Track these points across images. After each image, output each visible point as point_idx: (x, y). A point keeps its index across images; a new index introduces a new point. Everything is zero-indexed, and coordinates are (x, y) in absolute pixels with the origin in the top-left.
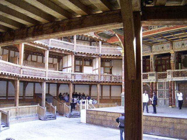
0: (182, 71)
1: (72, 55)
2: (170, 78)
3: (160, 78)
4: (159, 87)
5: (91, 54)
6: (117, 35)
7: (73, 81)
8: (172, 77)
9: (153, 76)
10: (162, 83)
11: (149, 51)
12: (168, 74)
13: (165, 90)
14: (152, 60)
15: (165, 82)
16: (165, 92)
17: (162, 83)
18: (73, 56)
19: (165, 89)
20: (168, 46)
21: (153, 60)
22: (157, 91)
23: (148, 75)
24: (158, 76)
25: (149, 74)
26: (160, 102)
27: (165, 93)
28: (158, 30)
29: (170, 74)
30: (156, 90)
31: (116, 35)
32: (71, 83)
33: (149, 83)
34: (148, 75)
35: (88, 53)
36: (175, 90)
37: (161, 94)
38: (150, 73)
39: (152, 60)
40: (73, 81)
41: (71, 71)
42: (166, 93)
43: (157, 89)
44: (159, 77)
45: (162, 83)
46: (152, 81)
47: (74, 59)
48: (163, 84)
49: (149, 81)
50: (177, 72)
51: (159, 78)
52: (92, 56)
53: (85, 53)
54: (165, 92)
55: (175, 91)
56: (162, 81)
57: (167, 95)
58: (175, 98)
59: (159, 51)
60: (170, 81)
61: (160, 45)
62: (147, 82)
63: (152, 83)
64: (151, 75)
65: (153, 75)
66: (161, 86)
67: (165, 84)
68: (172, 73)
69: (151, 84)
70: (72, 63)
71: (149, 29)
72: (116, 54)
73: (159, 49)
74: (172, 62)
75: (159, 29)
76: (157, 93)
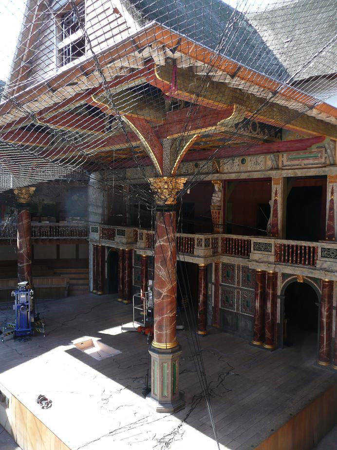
22: (133, 269)
43: (133, 265)
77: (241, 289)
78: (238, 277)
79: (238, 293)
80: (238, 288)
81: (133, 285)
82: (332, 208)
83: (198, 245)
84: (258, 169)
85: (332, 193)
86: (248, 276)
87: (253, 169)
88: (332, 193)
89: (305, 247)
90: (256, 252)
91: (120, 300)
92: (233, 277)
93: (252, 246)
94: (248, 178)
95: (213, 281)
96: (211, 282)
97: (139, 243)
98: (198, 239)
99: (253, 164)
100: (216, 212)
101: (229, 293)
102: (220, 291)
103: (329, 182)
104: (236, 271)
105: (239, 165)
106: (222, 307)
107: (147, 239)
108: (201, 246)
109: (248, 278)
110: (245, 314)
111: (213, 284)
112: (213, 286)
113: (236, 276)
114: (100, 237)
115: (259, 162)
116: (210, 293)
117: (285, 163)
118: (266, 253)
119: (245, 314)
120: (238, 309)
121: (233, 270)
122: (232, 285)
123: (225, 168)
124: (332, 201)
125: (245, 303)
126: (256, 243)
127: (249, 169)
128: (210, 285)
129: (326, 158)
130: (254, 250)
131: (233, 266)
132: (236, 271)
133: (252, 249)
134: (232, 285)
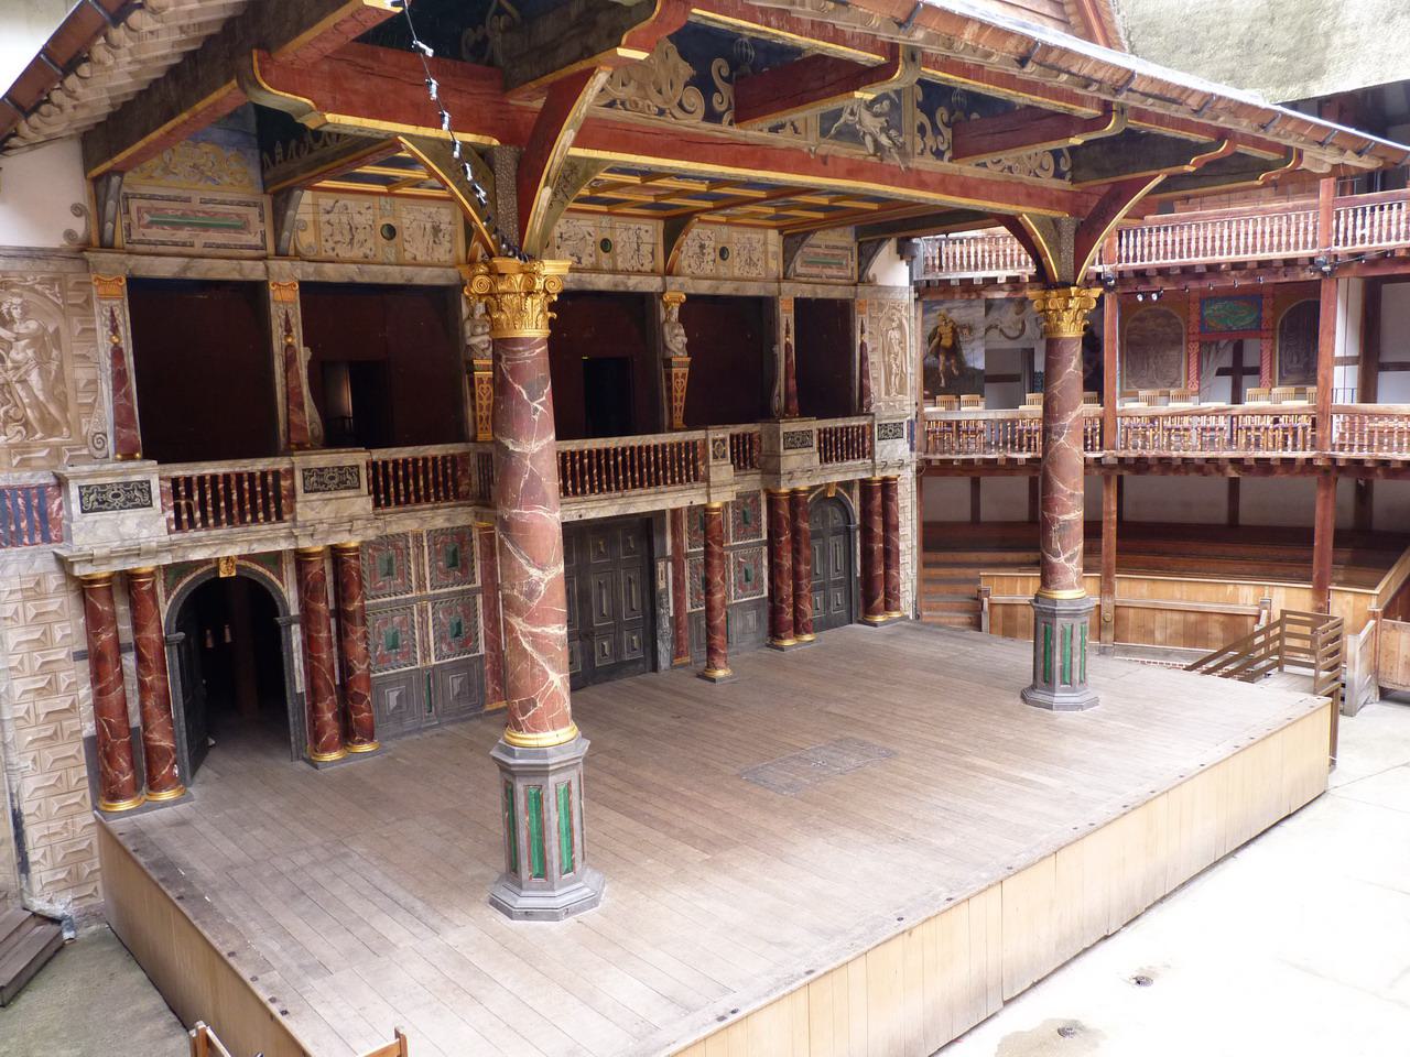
0: (599, 451)
9: (343, 485)
10: (396, 547)
11: (256, 240)
13: (428, 598)
14: (288, 330)
15: (418, 537)
16: (422, 611)
17: (396, 547)
19: (421, 586)
20: (436, 230)
21: (298, 331)
26: (393, 703)
27: (424, 623)
28: (824, 159)
38: (313, 465)
39: (288, 330)
48: (403, 553)
54: (422, 611)
57: (440, 639)
59: (357, 253)
61: (367, 201)
64: (320, 482)
66: (389, 573)
67: (420, 547)
73: (359, 236)
82: (864, 358)
83: (715, 457)
85: (862, 332)
86: (744, 513)
88: (862, 332)
89: (853, 427)
90: (789, 452)
94: (734, 293)
95: (669, 552)
96: (664, 557)
103: (860, 313)
105: (714, 261)
106: (692, 607)
108: (724, 456)
109: (745, 518)
111: (667, 559)
112: (670, 564)
114: (170, 532)
115: (755, 260)
116: (661, 585)
117: (800, 270)
118: (805, 450)
123: (685, 264)
124: (863, 345)
127: (737, 273)
128: (661, 566)
129: (852, 269)
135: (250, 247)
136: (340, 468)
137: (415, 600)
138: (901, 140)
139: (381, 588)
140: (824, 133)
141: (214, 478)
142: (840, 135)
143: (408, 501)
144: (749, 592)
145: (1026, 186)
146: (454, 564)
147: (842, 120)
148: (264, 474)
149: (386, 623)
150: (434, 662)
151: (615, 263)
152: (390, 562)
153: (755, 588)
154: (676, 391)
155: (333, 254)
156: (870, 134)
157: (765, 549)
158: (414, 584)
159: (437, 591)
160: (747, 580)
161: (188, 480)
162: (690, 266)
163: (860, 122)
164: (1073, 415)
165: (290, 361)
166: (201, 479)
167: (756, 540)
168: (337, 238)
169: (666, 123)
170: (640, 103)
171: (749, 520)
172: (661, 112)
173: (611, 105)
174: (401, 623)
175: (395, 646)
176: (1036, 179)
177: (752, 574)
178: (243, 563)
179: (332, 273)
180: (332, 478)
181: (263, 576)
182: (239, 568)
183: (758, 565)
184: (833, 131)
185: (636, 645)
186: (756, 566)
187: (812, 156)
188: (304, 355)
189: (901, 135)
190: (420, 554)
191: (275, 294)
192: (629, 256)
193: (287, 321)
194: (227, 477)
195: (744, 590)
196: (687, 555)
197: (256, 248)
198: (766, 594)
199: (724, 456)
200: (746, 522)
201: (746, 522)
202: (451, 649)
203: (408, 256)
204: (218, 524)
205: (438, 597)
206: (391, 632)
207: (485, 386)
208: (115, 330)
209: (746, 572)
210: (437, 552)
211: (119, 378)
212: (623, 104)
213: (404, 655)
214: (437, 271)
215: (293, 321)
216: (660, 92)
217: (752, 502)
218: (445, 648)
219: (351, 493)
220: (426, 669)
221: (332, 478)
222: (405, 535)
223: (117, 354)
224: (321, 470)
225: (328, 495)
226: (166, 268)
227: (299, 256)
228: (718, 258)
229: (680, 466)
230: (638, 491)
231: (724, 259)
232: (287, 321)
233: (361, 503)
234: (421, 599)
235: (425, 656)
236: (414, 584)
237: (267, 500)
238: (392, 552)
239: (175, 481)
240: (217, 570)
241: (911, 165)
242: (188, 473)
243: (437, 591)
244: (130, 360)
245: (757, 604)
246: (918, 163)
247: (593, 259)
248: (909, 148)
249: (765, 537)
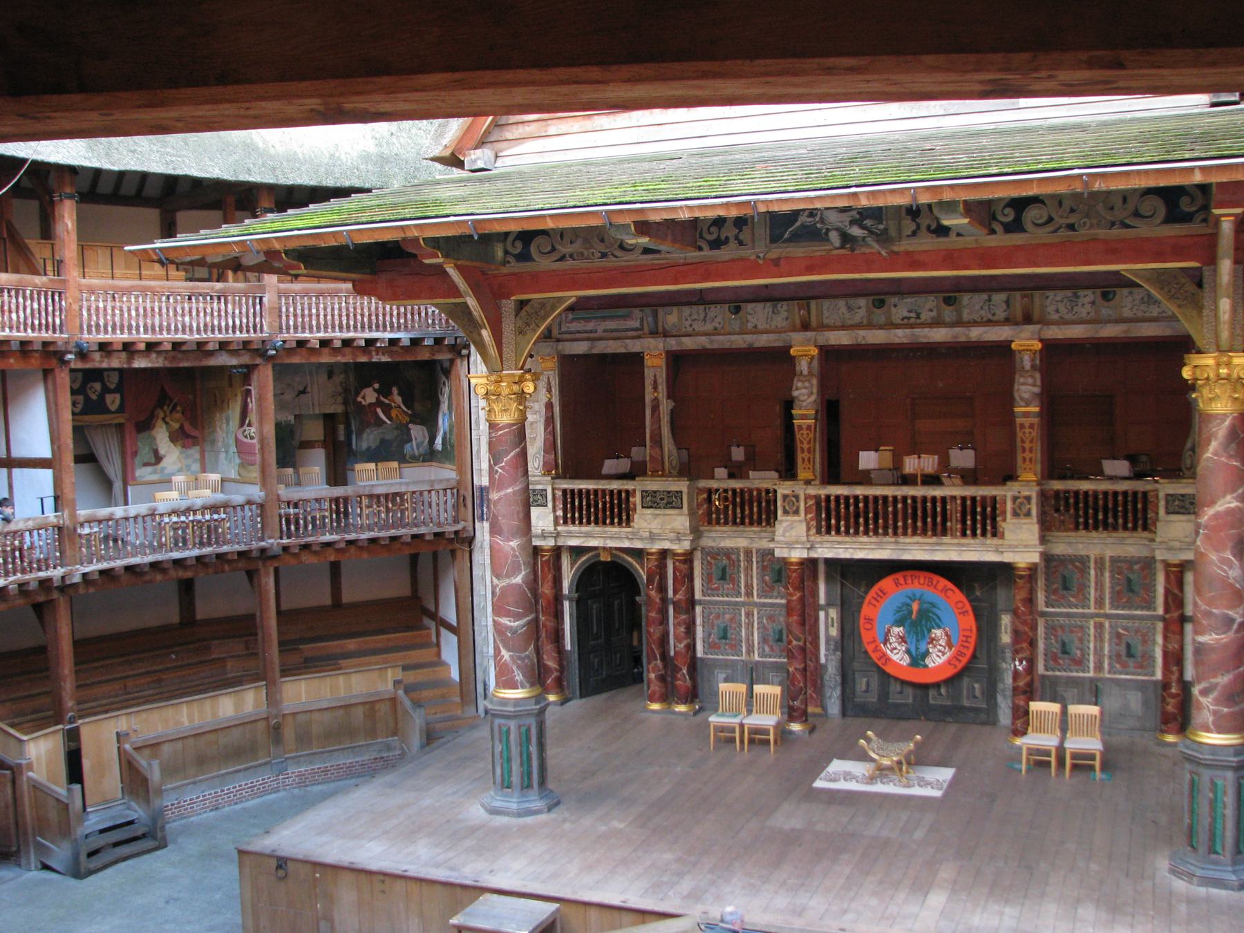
1: (47, 373)
2: (793, 538)
3: (718, 523)
4: (708, 578)
5: (201, 344)
6: (458, 267)
7: (77, 579)
8: (808, 529)
9: (669, 505)
10: (729, 558)
11: (637, 324)
12: (786, 512)
13: (756, 604)
14: (655, 388)
15: (748, 553)
17: (729, 558)
18: (63, 378)
19: (749, 594)
21: (662, 388)
22: (698, 609)
23: (637, 499)
24: (699, 506)
25: (638, 495)
27: (750, 625)
28: (776, 263)
29: (796, 512)
30: (691, 603)
31: (451, 271)
32: (55, 595)
33: (638, 554)
34: (637, 499)
35: (176, 345)
36: (824, 608)
37: (725, 630)
39: (655, 388)
40: (77, 579)
41: (49, 503)
42: (762, 627)
43: (698, 596)
44: (709, 513)
45: (728, 553)
46: (666, 545)
47: (66, 400)
48: (735, 564)
49: (638, 545)
50: (847, 498)
51: (710, 523)
52: (212, 362)
53: (151, 346)
55: (822, 614)
56: (728, 543)
57: (764, 640)
58: (823, 660)
59: (709, 327)
60: (797, 554)
62: (626, 544)
63: (664, 553)
64: (654, 501)
65: (670, 501)
66: (723, 578)
67: (749, 561)
68: (811, 502)
69: (653, 563)
70: (55, 438)
71: (705, 246)
72: (388, 335)
74: (804, 417)
75: (776, 252)
76: (699, 620)
77: (1107, 616)
78: (1099, 586)
79: (1099, 626)
80: (1097, 615)
81: (700, 654)
84: (1155, 314)
86: (1129, 581)
87: (1140, 314)
91: (655, 706)
92: (1083, 588)
93: (1162, 504)
97: (785, 524)
98: (1015, 499)
99: (1137, 302)
100: (1032, 426)
101: (1072, 632)
102: (1041, 630)
104: (1092, 572)
105: (1093, 303)
106: (1047, 669)
107: (807, 512)
108: (1028, 514)
110: (1123, 677)
113: (1093, 584)
114: (556, 523)
119: (1123, 677)
120: (1099, 668)
121: (1084, 571)
122: (1081, 610)
123: (1051, 309)
125: (1123, 649)
126: (1172, 495)
127: (1127, 313)
130: (1168, 513)
131: (1084, 560)
132: (1092, 572)
133: (1162, 511)
134: (1081, 610)
135: (632, 330)
136: (669, 492)
137: (743, 604)
138: (881, 227)
139: (717, 589)
140: (775, 239)
141: (588, 491)
142: (796, 238)
143: (743, 523)
144: (1131, 670)
145: (1105, 241)
146: (779, 581)
147: (798, 224)
148: (620, 492)
149: (718, 617)
150: (757, 658)
151: (959, 314)
152: (724, 570)
153: (1141, 667)
154: (1023, 441)
155: (690, 329)
156: (837, 229)
157: (1160, 625)
158: (743, 590)
159: (763, 600)
160: (1130, 655)
161: (572, 491)
162: (1057, 311)
163: (822, 221)
164: (1210, 512)
165: (655, 408)
166: (580, 491)
167: (1145, 613)
168: (695, 317)
169: (611, 262)
170: (586, 253)
171: (1136, 588)
172: (604, 255)
173: (562, 259)
174: (732, 620)
175: (725, 637)
176: (1124, 230)
177: (1138, 649)
178: (617, 553)
179: (689, 343)
180: (662, 499)
181: (631, 565)
182: (612, 555)
183: (1147, 640)
184: (786, 236)
185: (978, 693)
186: (1144, 642)
187: (761, 262)
188: (666, 406)
189: (881, 223)
190: (749, 568)
191: (648, 361)
192: (977, 307)
193: (655, 382)
194: (596, 491)
195: (1124, 665)
196: (1043, 614)
197: (636, 330)
198: (1159, 675)
199: (1028, 514)
200: (1131, 591)
201: (1131, 591)
202: (772, 650)
203: (750, 326)
204: (589, 523)
205: (764, 605)
206: (722, 625)
207: (805, 432)
208: (549, 390)
209: (1128, 646)
210: (764, 568)
211: (549, 421)
212: (571, 256)
213: (732, 646)
214: (772, 336)
215: (659, 381)
216: (602, 241)
217: (1143, 569)
218: (767, 649)
219: (676, 511)
220: (751, 662)
221: (662, 499)
222: (738, 549)
223: (549, 406)
224: (655, 492)
225: (657, 511)
226: (580, 348)
227: (666, 335)
228: (1099, 301)
229: (974, 521)
230: (917, 539)
231: (1109, 300)
232: (655, 382)
233: (679, 521)
234: (749, 604)
235: (750, 651)
236: (743, 590)
237: (616, 510)
238: (725, 561)
239: (564, 491)
240: (598, 555)
241: (895, 249)
242: (571, 487)
243: (763, 600)
244: (557, 410)
245: (1141, 686)
246: (904, 246)
247: (934, 314)
248: (893, 232)
249: (1160, 611)
